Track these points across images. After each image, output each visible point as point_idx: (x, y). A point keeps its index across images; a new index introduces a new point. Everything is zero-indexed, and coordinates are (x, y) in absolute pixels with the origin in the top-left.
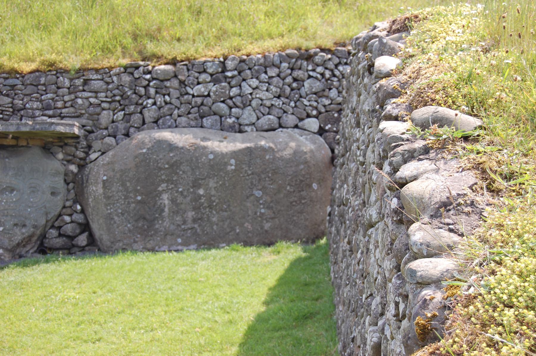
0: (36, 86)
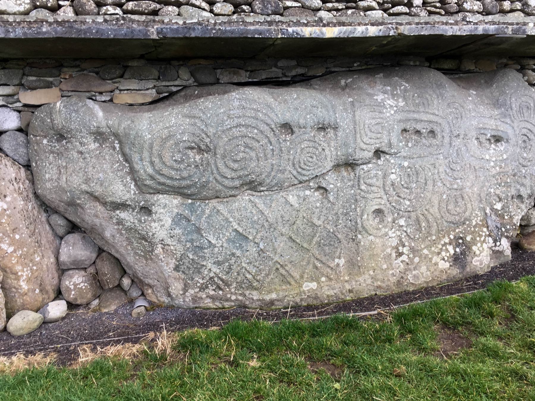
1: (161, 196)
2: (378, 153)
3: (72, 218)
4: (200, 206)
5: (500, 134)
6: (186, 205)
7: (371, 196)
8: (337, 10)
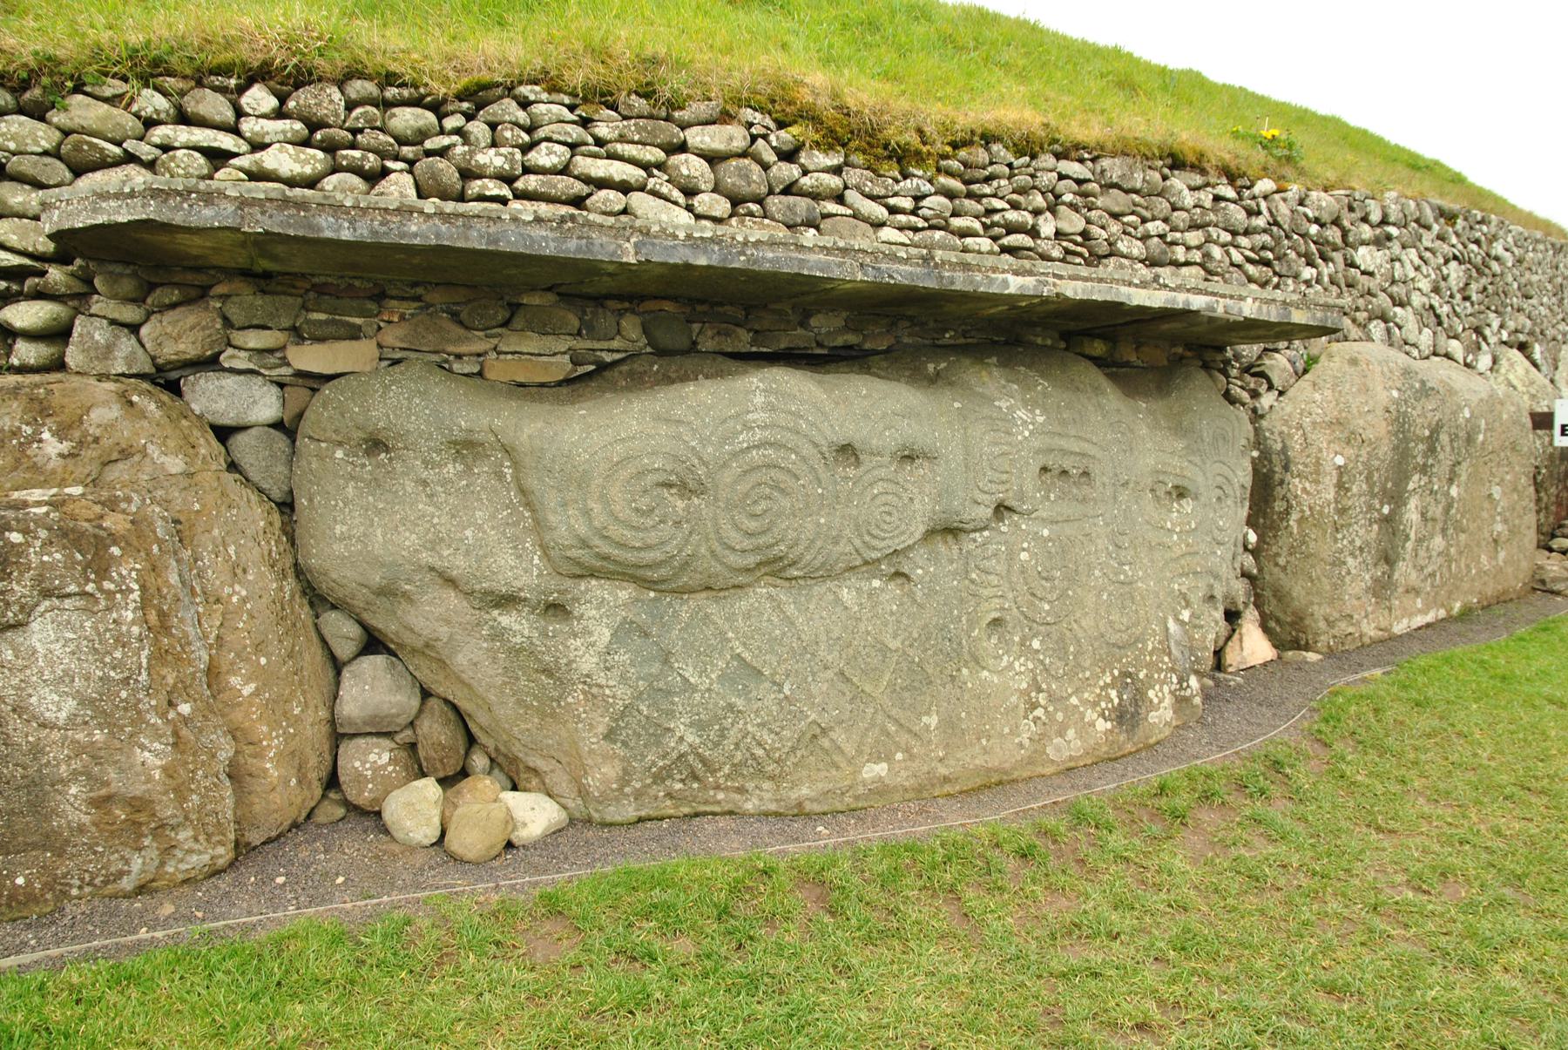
0: (1127, 192)
1: (594, 582)
2: (1002, 509)
3: (378, 622)
4: (670, 604)
5: (1185, 483)
6: (643, 601)
7: (986, 592)
8: (916, 230)
